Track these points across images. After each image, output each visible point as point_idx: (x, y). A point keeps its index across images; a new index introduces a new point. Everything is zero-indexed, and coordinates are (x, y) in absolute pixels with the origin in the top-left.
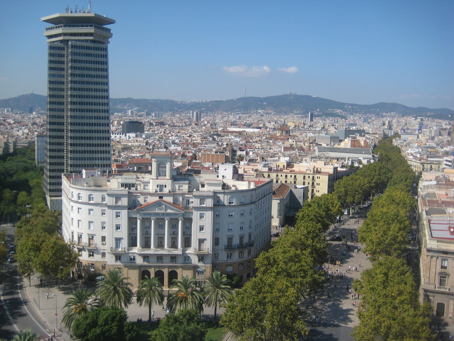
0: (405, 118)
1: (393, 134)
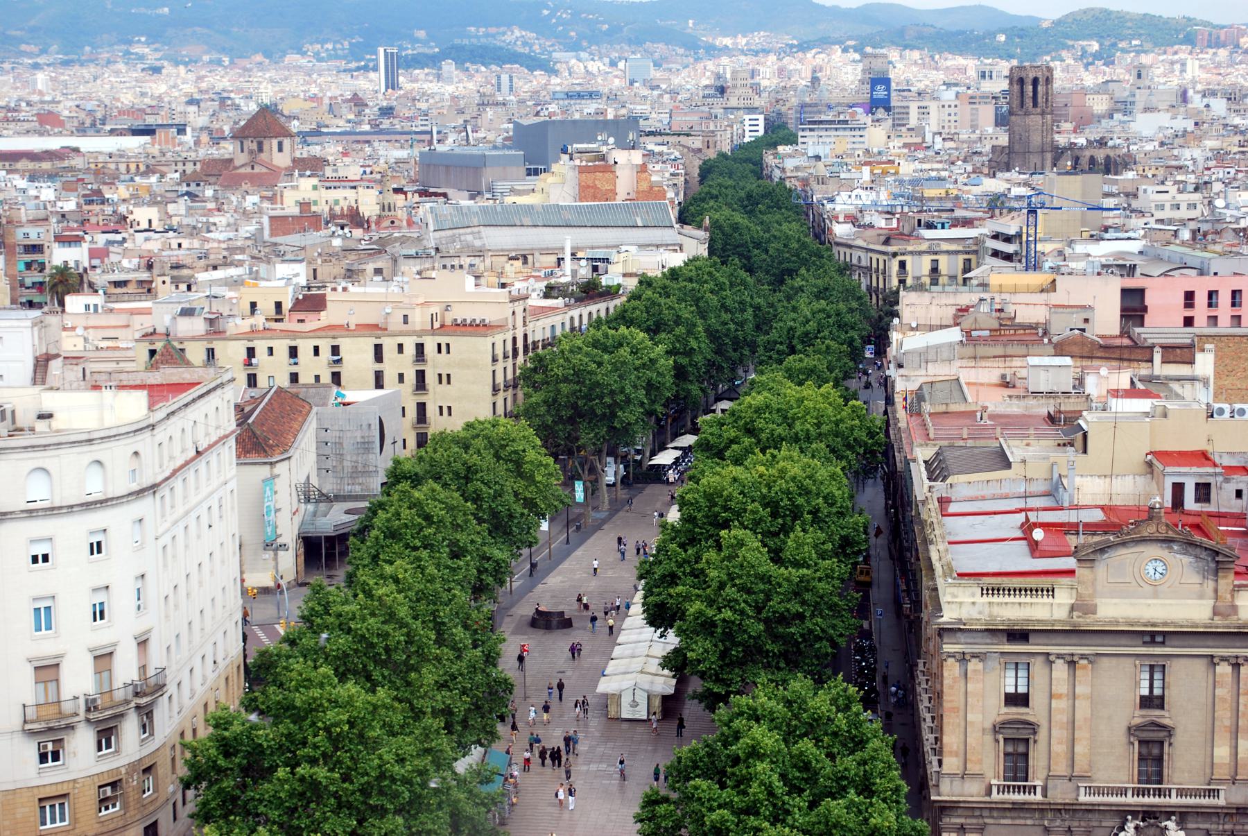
0: (809, 55)
1: (761, 133)
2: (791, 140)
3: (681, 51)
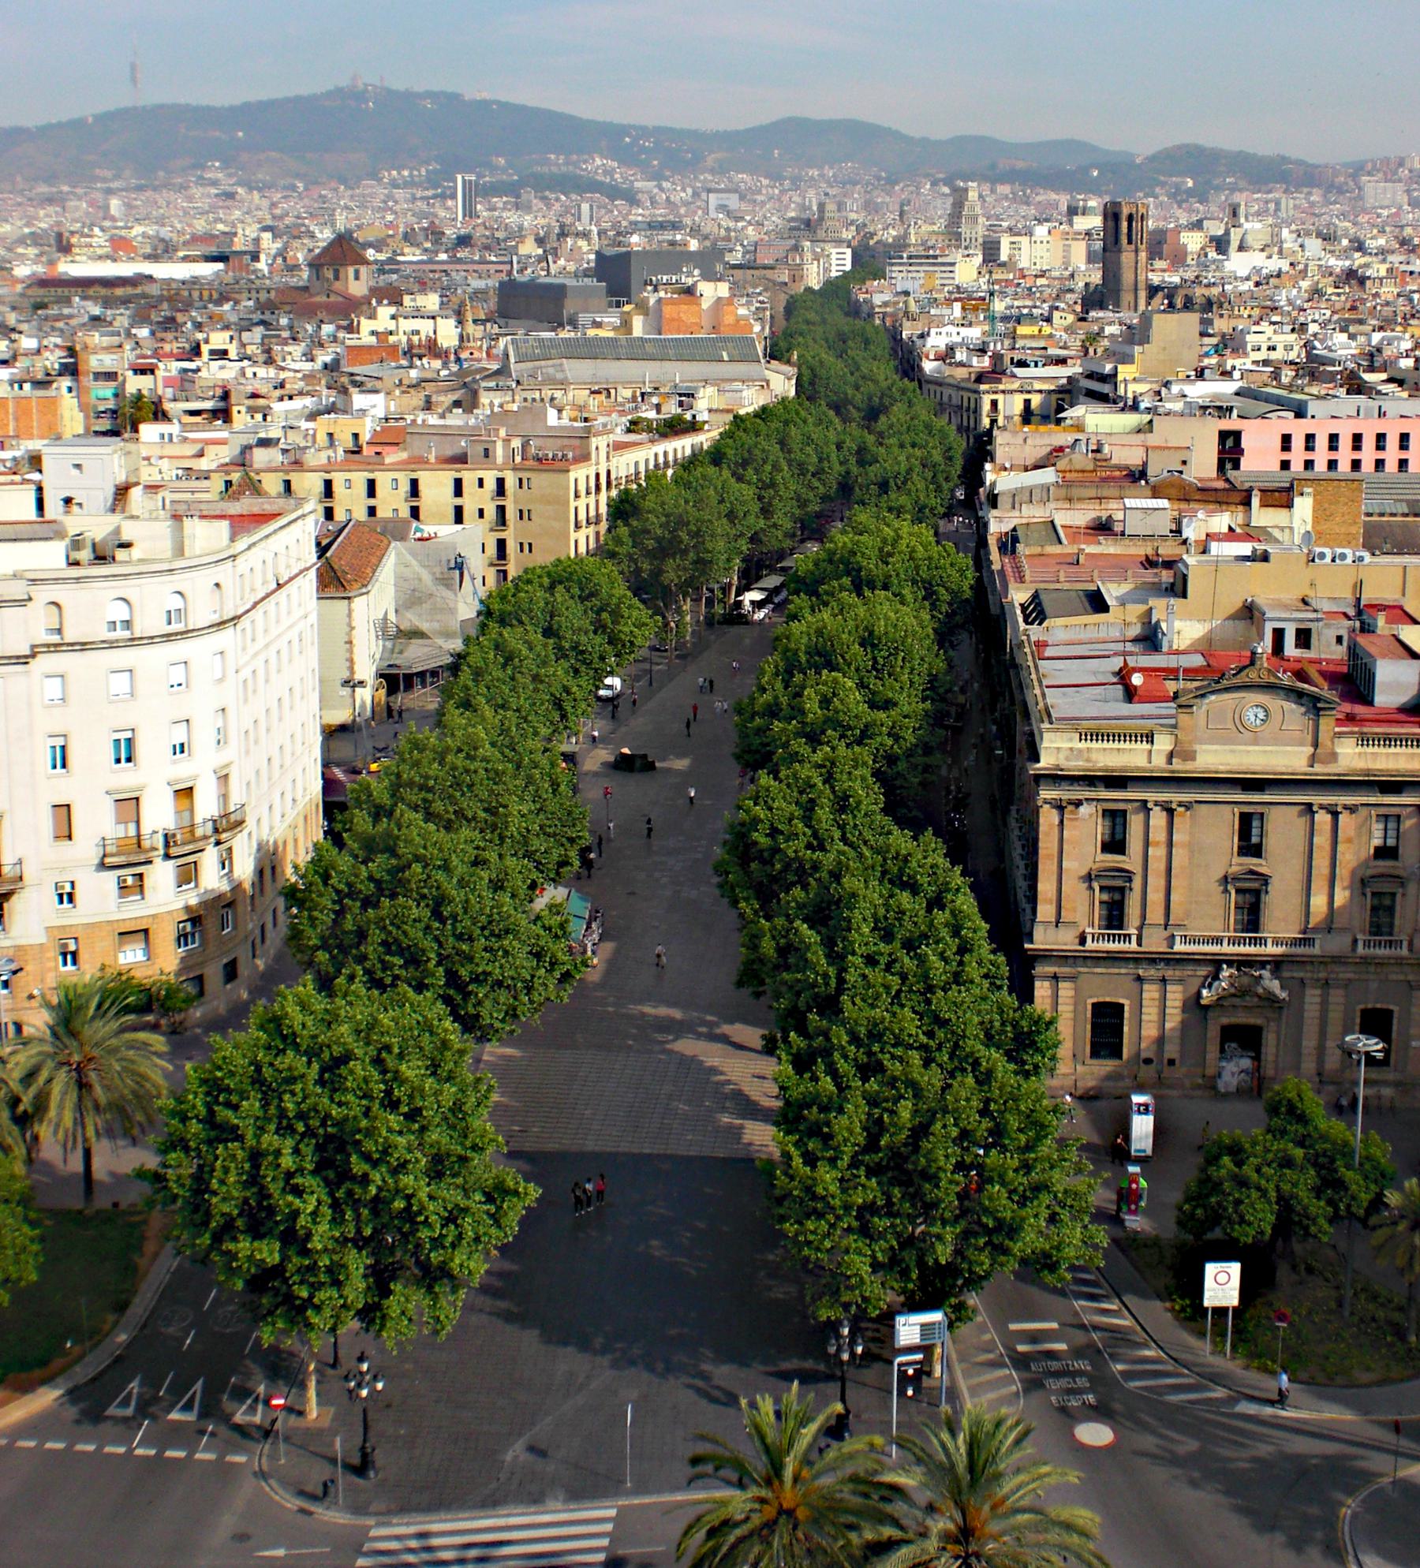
1: (848, 268)
2: (879, 274)
3: (765, 182)
